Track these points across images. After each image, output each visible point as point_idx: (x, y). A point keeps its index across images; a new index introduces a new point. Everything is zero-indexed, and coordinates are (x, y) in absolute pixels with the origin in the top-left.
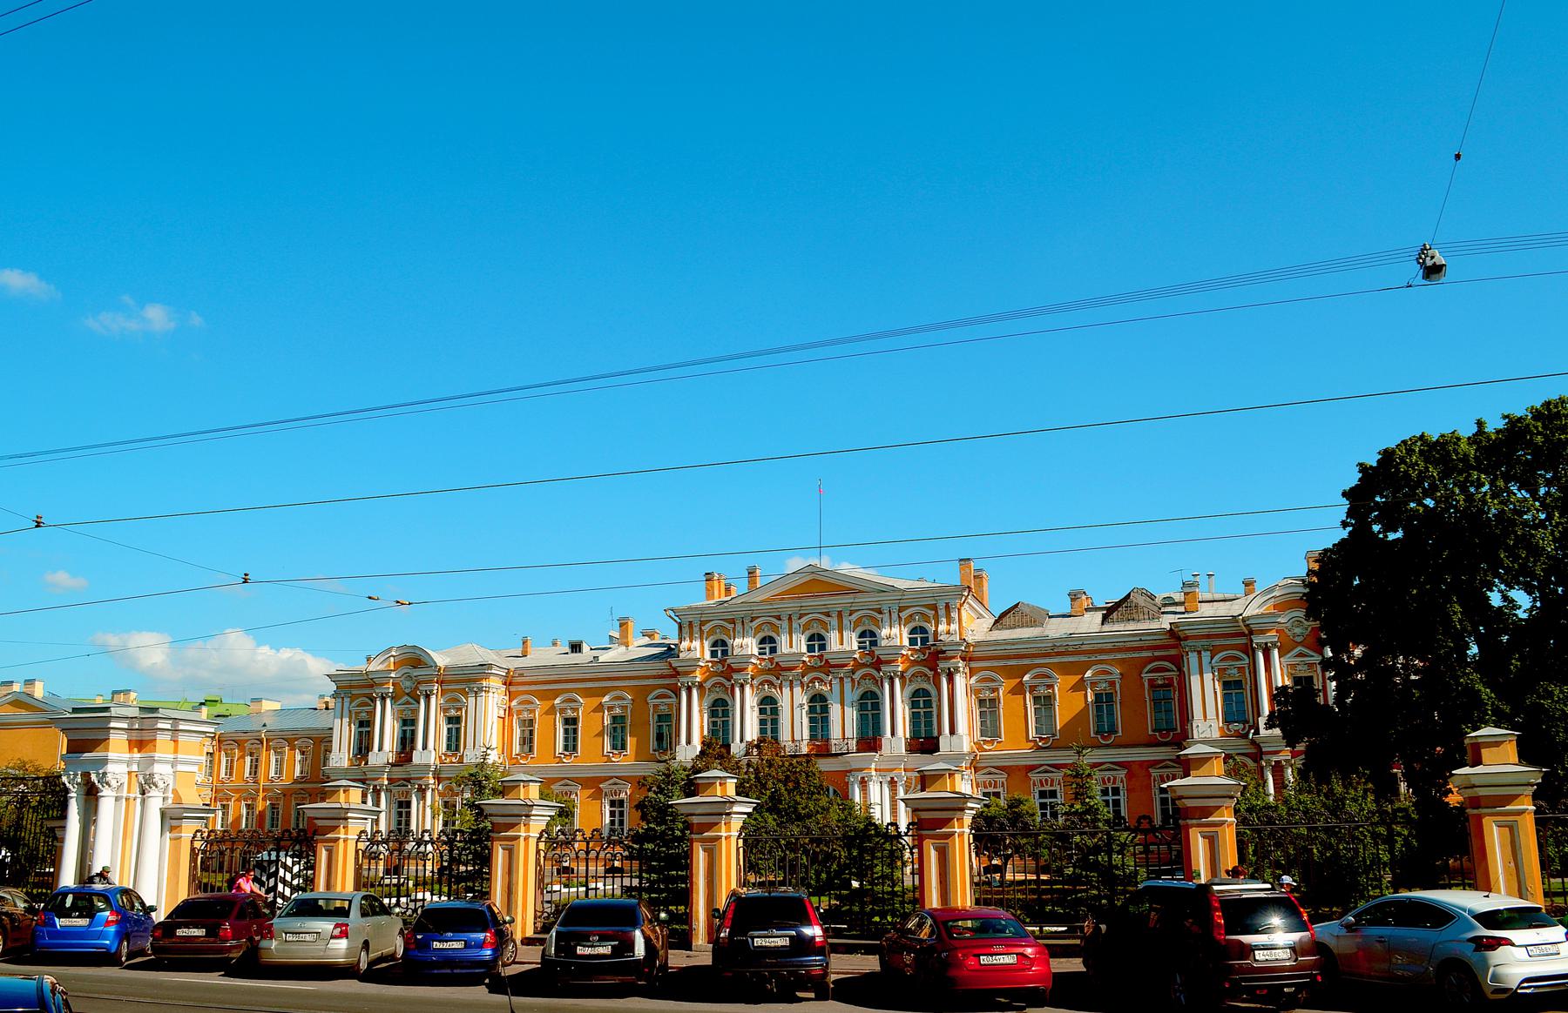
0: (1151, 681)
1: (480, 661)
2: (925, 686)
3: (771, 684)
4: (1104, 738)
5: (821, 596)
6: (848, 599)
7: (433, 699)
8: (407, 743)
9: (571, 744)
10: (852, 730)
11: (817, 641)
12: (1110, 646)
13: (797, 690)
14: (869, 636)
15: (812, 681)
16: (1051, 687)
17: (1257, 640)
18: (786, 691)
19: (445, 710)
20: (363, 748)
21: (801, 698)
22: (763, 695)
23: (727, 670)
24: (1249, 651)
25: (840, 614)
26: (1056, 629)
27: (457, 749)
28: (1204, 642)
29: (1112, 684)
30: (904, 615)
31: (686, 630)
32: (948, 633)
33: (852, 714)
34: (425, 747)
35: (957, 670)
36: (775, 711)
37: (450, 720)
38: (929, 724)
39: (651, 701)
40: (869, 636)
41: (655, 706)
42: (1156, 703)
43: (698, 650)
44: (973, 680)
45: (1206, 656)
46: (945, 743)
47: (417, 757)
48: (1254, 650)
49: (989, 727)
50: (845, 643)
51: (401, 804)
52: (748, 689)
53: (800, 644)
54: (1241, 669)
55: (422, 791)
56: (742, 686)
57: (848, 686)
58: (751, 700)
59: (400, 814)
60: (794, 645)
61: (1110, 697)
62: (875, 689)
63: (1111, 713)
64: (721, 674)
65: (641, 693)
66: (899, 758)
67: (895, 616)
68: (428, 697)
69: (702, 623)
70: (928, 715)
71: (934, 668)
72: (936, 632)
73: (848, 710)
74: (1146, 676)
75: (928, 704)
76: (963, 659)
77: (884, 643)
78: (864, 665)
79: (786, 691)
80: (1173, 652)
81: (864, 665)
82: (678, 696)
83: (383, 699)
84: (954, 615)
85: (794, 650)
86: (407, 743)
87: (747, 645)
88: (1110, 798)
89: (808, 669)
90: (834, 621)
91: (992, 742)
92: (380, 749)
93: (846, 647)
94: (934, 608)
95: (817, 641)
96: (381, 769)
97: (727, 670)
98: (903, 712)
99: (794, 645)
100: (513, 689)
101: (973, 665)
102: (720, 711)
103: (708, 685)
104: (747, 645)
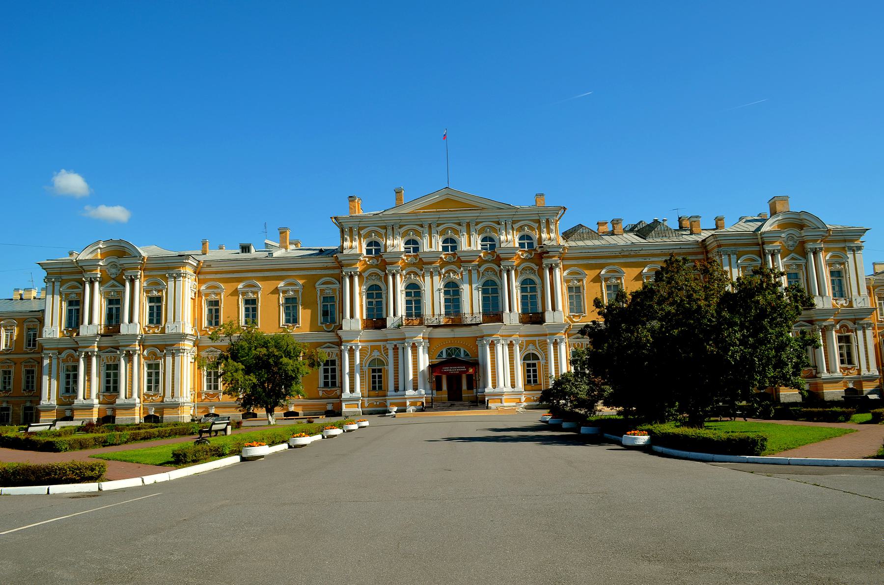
2: (532, 277)
3: (416, 274)
5: (454, 212)
6: (475, 214)
7: (137, 283)
8: (114, 317)
10: (478, 308)
11: (451, 243)
13: (436, 278)
15: (448, 272)
16: (620, 278)
17: (768, 248)
18: (428, 279)
19: (147, 292)
20: (75, 319)
21: (439, 283)
22: (409, 282)
23: (381, 262)
25: (468, 225)
27: (159, 322)
28: (733, 248)
30: (516, 226)
32: (550, 239)
33: (478, 296)
34: (131, 320)
35: (557, 265)
36: (418, 294)
37: (151, 300)
38: (534, 304)
39: (319, 287)
40: (490, 242)
43: (357, 247)
44: (565, 273)
46: (549, 317)
47: (124, 329)
48: (765, 255)
49: (576, 307)
50: (471, 244)
51: (108, 367)
52: (398, 277)
53: (438, 244)
55: (129, 357)
56: (394, 276)
57: (475, 276)
58: (401, 286)
59: (108, 375)
60: (432, 245)
64: (377, 266)
65: (312, 281)
66: (515, 328)
67: (509, 226)
68: (132, 281)
69: (360, 229)
70: (534, 297)
71: (540, 265)
73: (475, 292)
75: (533, 289)
78: (486, 261)
79: (428, 279)
81: (486, 261)
83: (92, 283)
84: (552, 227)
85: (433, 249)
86: (114, 317)
87: (397, 244)
89: (444, 264)
90: (464, 229)
91: (579, 316)
92: (91, 322)
93: (473, 248)
94: (539, 222)
95: (451, 243)
96: (91, 339)
97: (381, 262)
98: (517, 294)
99: (432, 245)
100: (201, 277)
102: (376, 295)
103: (365, 275)
104: (397, 244)
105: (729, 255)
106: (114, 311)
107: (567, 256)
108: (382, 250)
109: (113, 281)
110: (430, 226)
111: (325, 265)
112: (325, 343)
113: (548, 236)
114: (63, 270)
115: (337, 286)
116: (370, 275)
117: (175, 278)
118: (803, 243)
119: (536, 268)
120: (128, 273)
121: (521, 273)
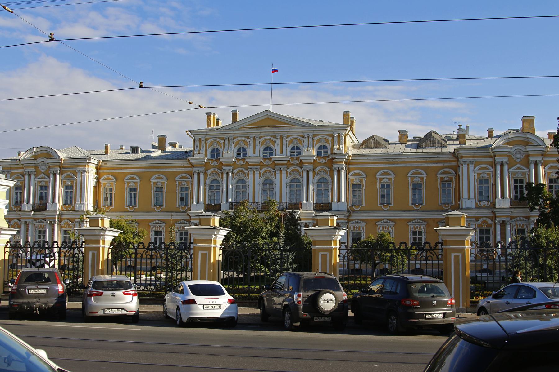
0: (441, 178)
1: (83, 156)
2: (325, 176)
4: (416, 206)
9: (133, 201)
12: (422, 160)
14: (296, 150)
15: (265, 172)
17: (498, 159)
21: (259, 181)
24: (494, 165)
25: (281, 137)
26: (392, 150)
27: (71, 203)
28: (471, 159)
29: (422, 179)
31: (197, 143)
32: (339, 149)
35: (342, 169)
36: (245, 186)
41: (180, 183)
42: (443, 188)
45: (471, 167)
48: (495, 165)
51: (40, 232)
54: (488, 174)
61: (420, 185)
62: (298, 177)
63: (420, 194)
64: (216, 167)
72: (332, 149)
74: (439, 176)
76: (346, 163)
77: (305, 153)
80: (454, 164)
81: (293, 165)
82: (192, 177)
88: (417, 237)
94: (332, 136)
101: (351, 166)
105: (468, 165)
106: (44, 195)
107: (353, 161)
108: (221, 155)
109: (42, 175)
110: (254, 138)
111: (183, 165)
112: (181, 220)
113: (337, 147)
114: (12, 166)
115: (190, 180)
116: (212, 173)
117: (82, 173)
118: (528, 156)
119: (328, 170)
120: (52, 169)
121: (318, 173)
